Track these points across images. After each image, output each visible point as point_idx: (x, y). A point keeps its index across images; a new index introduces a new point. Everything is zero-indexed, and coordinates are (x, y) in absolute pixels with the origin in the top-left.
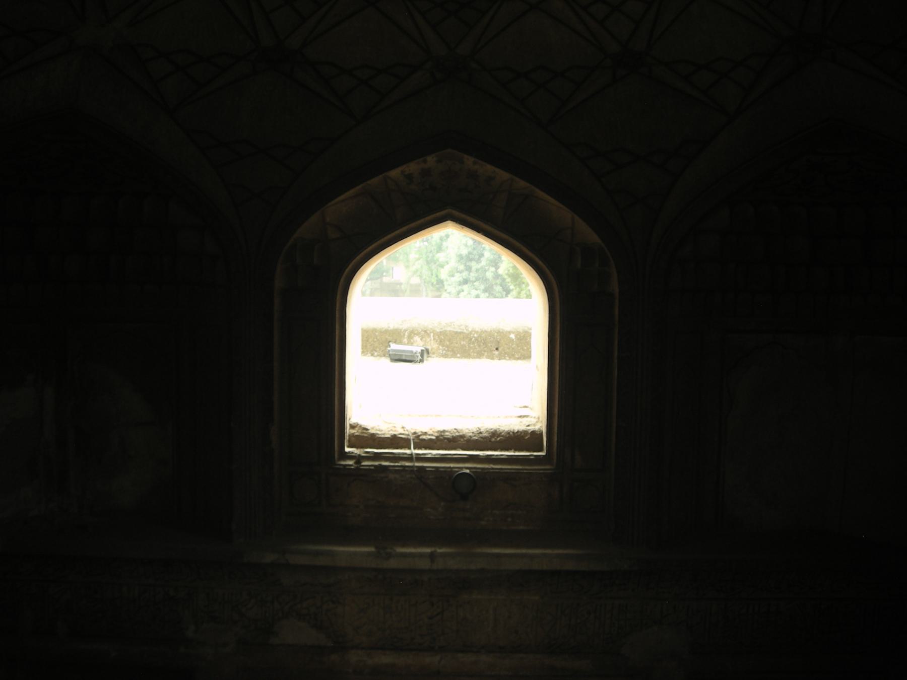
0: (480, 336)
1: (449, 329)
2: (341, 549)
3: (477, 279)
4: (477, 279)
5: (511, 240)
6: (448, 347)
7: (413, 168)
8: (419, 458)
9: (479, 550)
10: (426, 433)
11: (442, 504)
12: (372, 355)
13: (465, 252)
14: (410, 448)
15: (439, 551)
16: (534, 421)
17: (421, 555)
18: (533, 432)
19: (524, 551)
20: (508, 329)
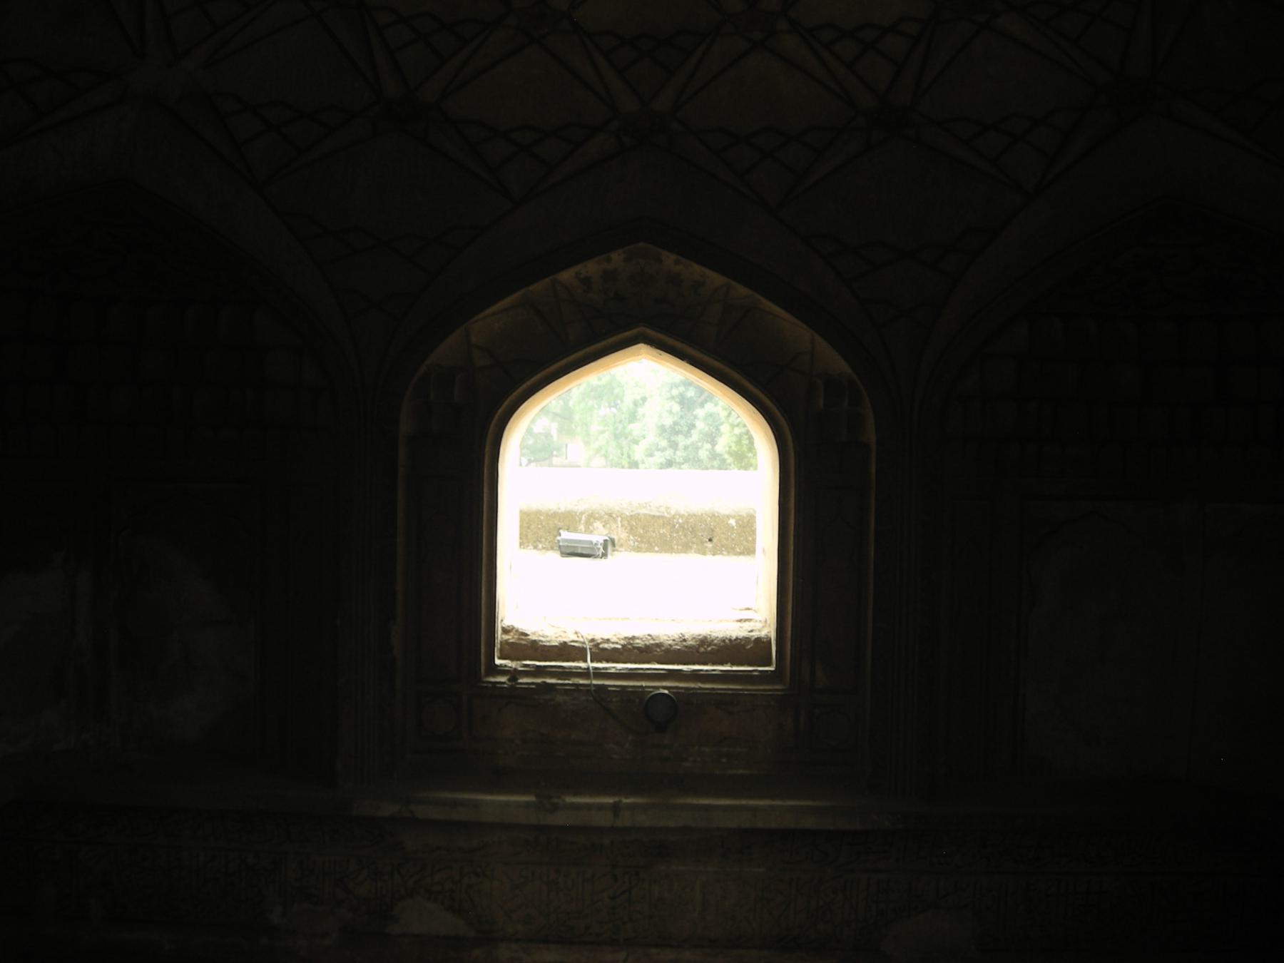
0: (687, 522)
1: (643, 511)
2: (489, 797)
3: (686, 460)
4: (686, 460)
5: (727, 370)
6: (641, 536)
7: (591, 268)
8: (599, 674)
9: (681, 801)
10: (608, 641)
12: (535, 547)
13: (668, 421)
14: (585, 661)
15: (625, 801)
16: (759, 625)
17: (601, 807)
18: (758, 640)
19: (744, 802)
20: (727, 513)
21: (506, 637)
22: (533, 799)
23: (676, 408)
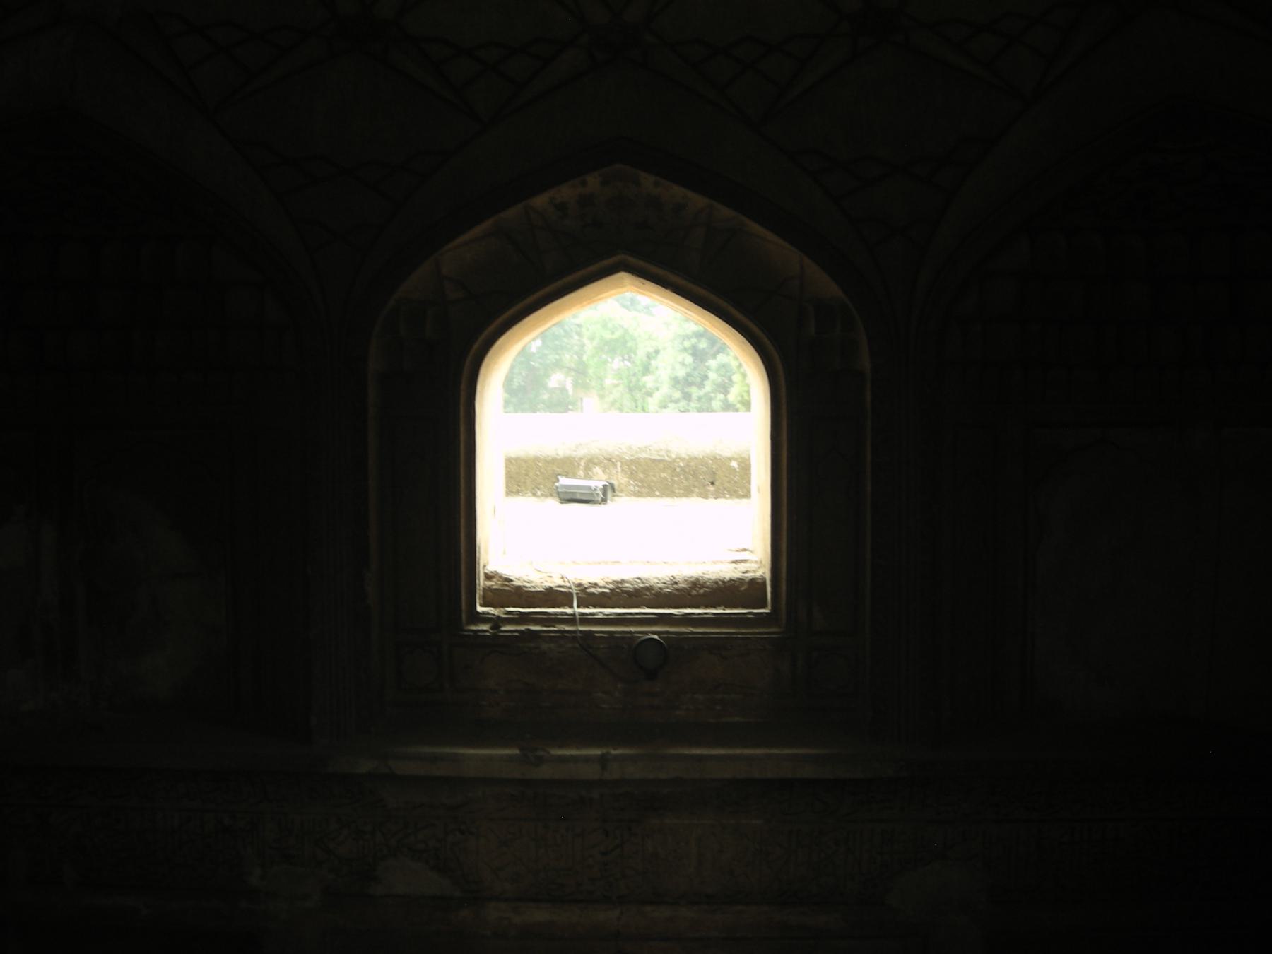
1: (644, 455)
2: (472, 751)
5: (713, 297)
6: (641, 481)
7: (566, 192)
8: (585, 620)
9: (672, 751)
10: (595, 585)
11: (620, 686)
12: (534, 495)
13: (681, 373)
14: (571, 607)
15: (613, 752)
16: (754, 566)
17: (587, 759)
18: (753, 581)
19: (738, 751)
20: (729, 455)
21: (489, 583)
22: (517, 752)
23: (689, 359)
